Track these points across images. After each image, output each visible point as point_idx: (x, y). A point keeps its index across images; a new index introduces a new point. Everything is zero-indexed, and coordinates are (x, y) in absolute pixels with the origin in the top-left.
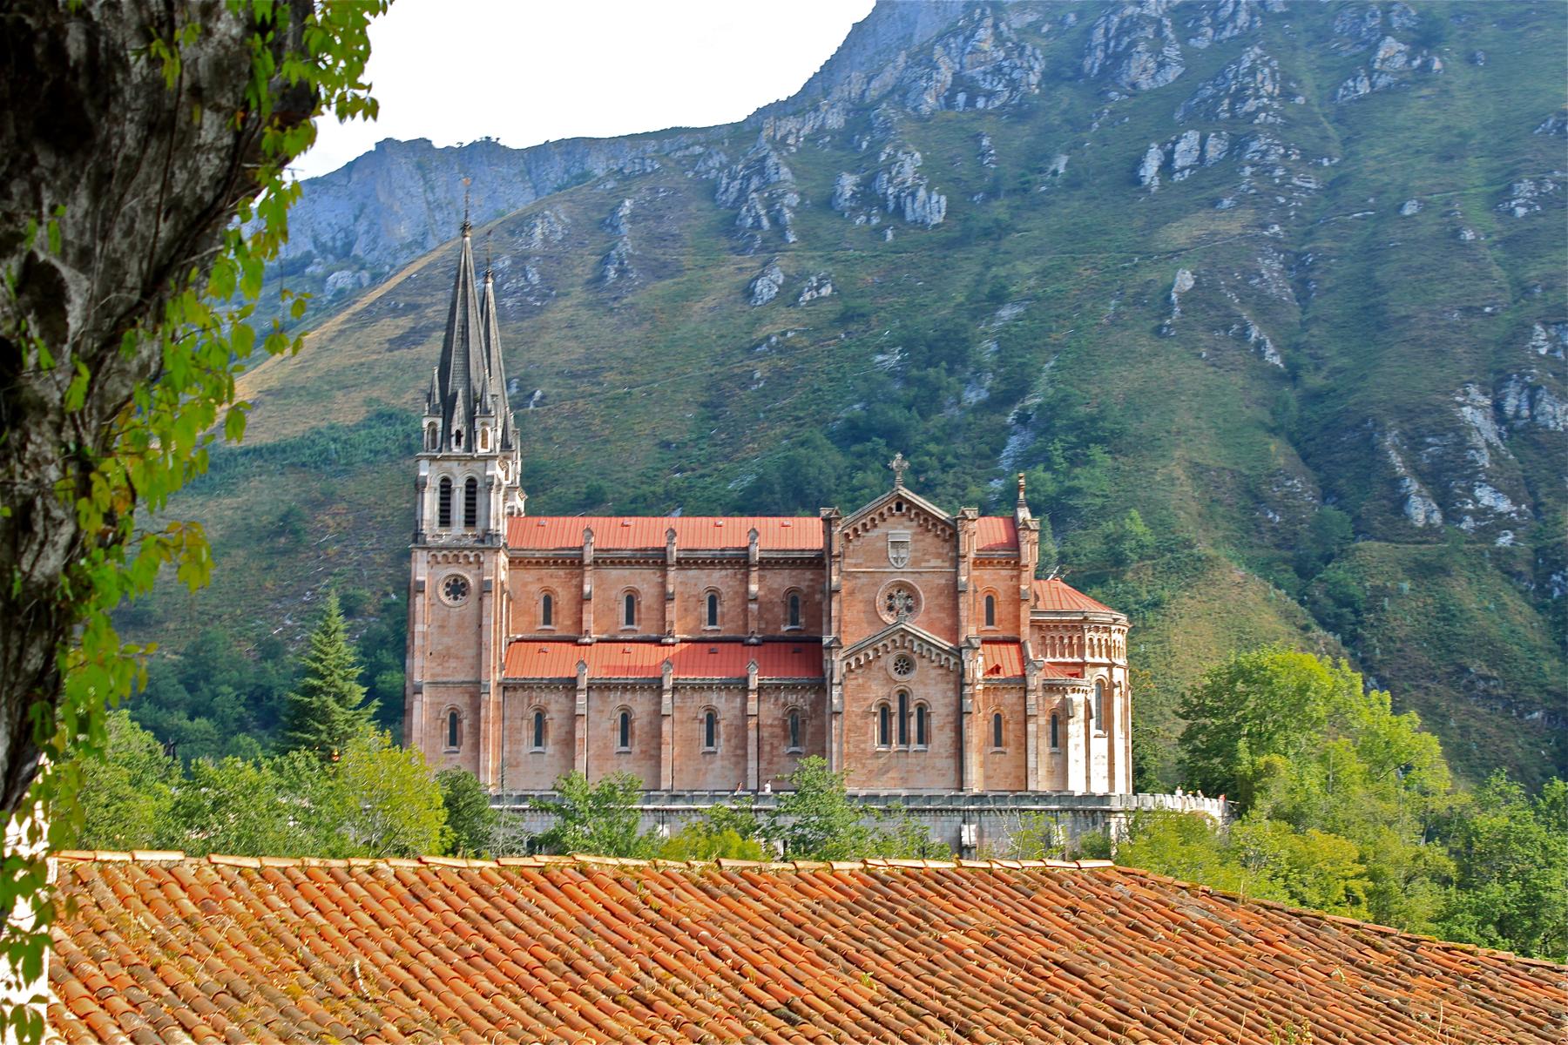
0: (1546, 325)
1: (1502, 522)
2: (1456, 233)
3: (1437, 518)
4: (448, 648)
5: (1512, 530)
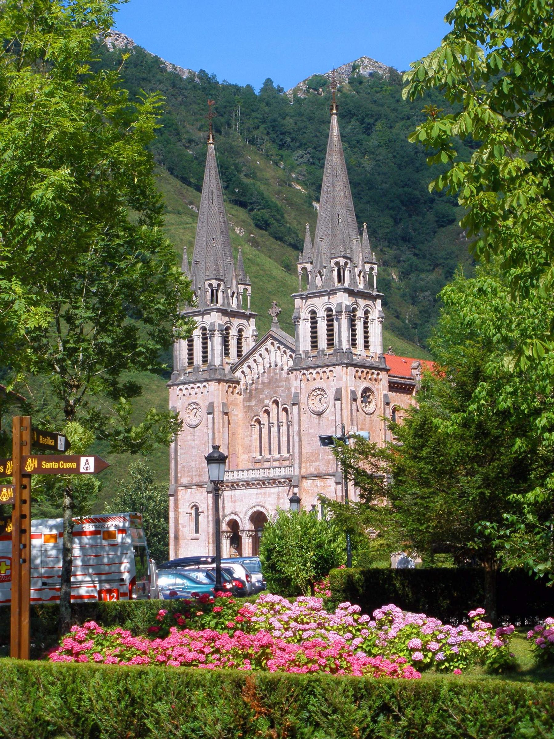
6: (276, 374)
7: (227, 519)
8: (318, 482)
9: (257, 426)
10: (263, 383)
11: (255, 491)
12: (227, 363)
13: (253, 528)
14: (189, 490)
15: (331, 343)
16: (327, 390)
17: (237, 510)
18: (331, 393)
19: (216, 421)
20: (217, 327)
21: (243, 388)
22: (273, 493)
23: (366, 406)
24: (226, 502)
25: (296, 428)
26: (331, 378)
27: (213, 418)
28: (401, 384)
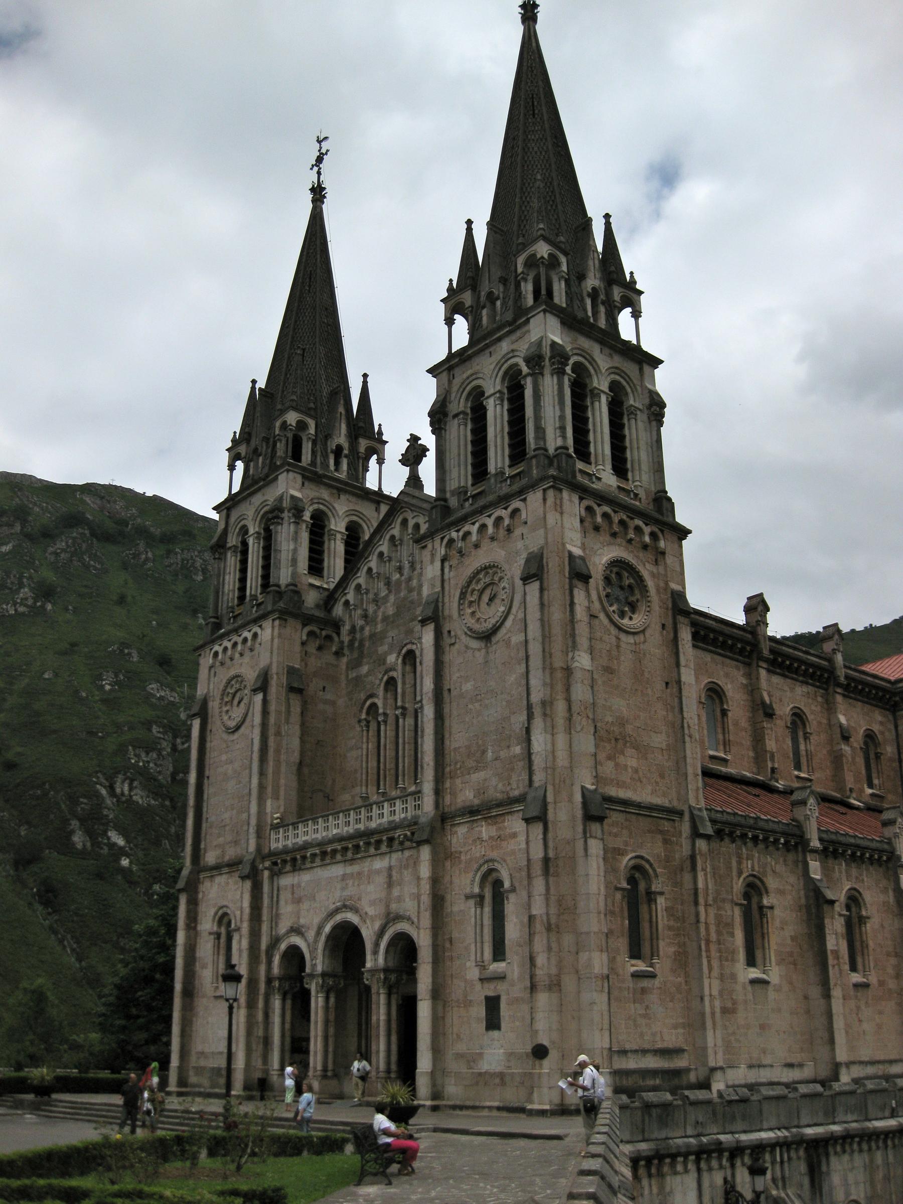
0: (134, 747)
1: (122, 852)
2: (77, 692)
3: (88, 844)
4: (622, 722)
5: (128, 857)
6: (410, 590)
7: (283, 946)
8: (485, 831)
9: (373, 726)
10: (385, 619)
11: (337, 870)
12: (312, 585)
13: (339, 970)
14: (218, 880)
15: (518, 449)
16: (505, 567)
17: (302, 921)
18: (516, 569)
19: (272, 707)
20: (286, 504)
21: (346, 639)
22: (378, 872)
23: (622, 615)
24: (282, 903)
25: (428, 684)
26: (517, 532)
27: (265, 702)
28: (722, 633)
